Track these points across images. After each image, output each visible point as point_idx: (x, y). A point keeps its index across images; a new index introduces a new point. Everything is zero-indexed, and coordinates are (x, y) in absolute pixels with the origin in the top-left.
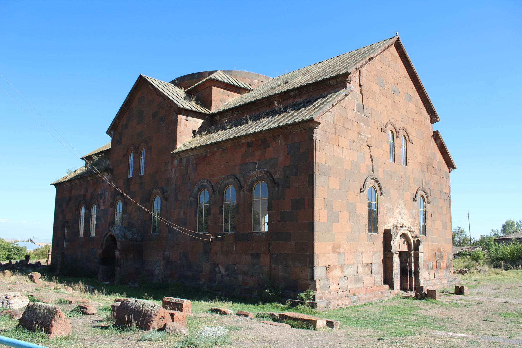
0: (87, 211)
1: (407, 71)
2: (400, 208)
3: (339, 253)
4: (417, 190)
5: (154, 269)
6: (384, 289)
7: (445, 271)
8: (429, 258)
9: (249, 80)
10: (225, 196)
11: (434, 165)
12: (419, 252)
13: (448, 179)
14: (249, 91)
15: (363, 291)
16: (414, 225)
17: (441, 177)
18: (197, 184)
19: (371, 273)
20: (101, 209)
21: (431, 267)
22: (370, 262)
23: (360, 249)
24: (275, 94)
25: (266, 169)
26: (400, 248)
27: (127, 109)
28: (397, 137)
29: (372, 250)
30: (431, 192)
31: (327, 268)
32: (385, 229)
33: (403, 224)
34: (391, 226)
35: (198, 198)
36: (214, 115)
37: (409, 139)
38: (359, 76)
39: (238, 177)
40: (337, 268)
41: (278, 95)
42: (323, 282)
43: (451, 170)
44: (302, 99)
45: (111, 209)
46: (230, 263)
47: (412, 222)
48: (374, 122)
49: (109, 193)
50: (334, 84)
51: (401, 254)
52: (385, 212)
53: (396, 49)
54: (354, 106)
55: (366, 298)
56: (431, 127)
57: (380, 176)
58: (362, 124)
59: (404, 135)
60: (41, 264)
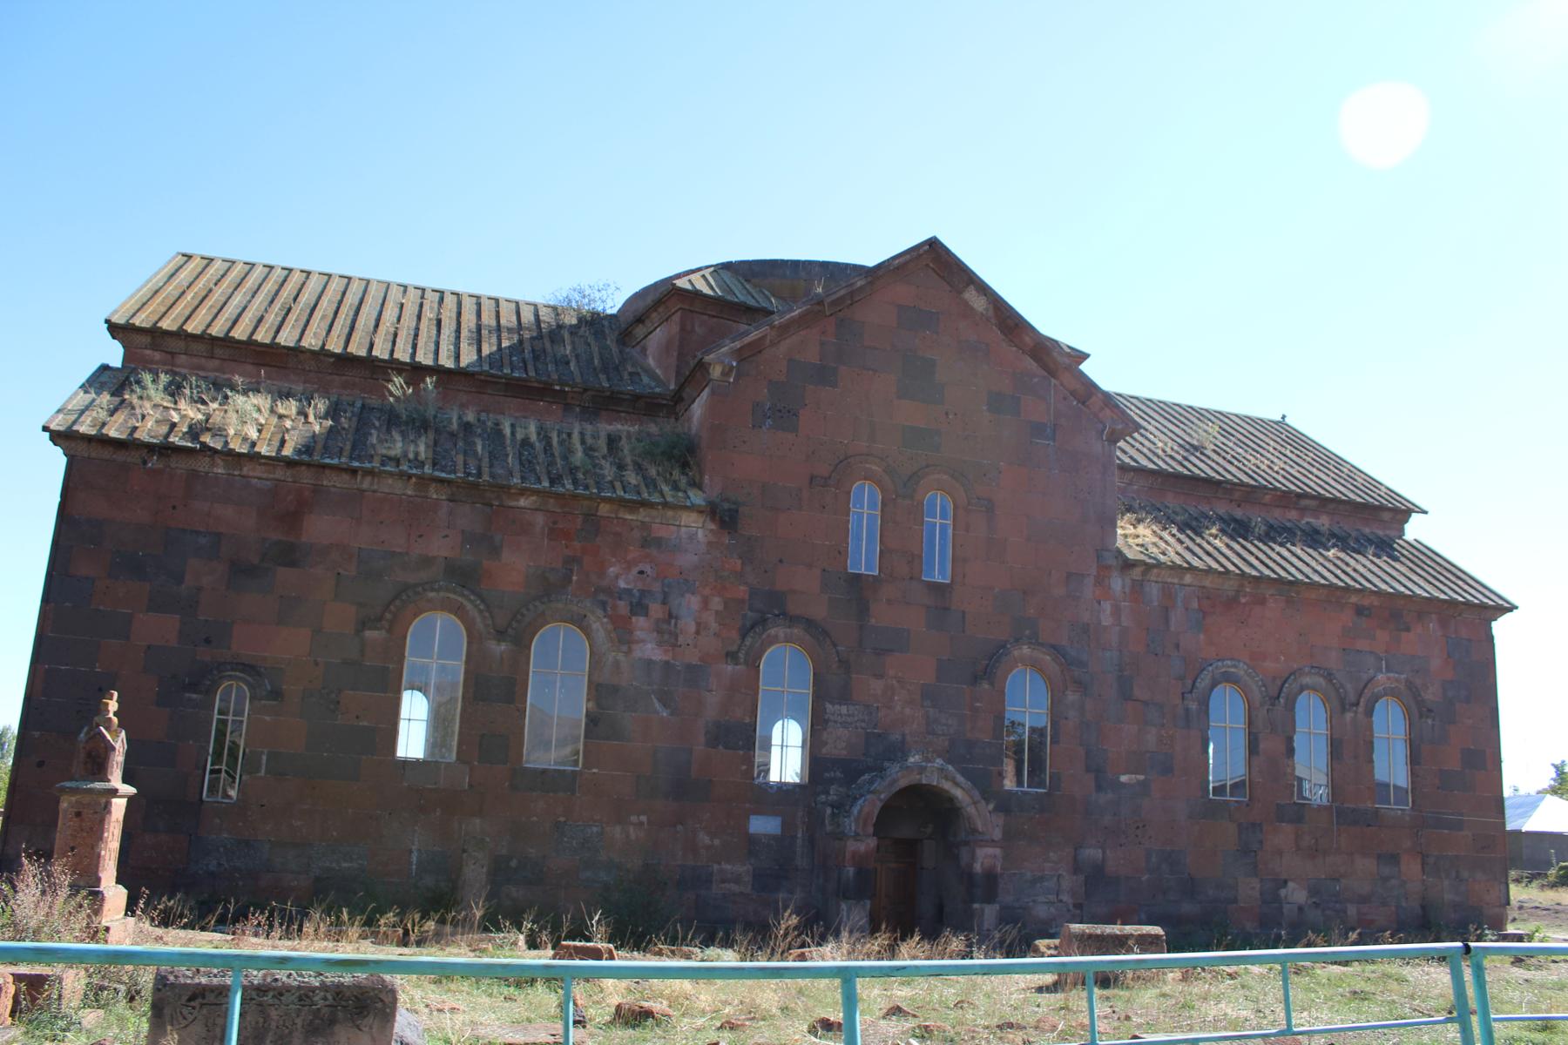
27: (828, 314)
46: (1323, 877)
49: (705, 603)
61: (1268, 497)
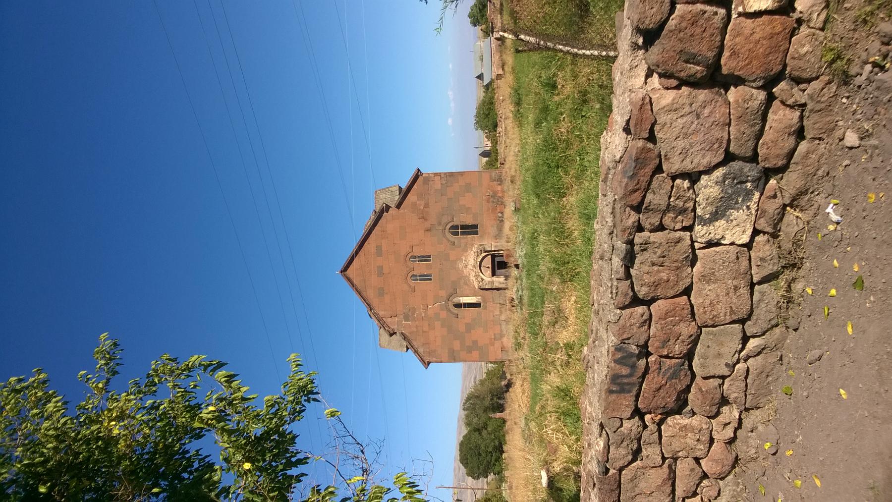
3: (495, 339)
11: (422, 207)
13: (427, 180)
23: (492, 318)
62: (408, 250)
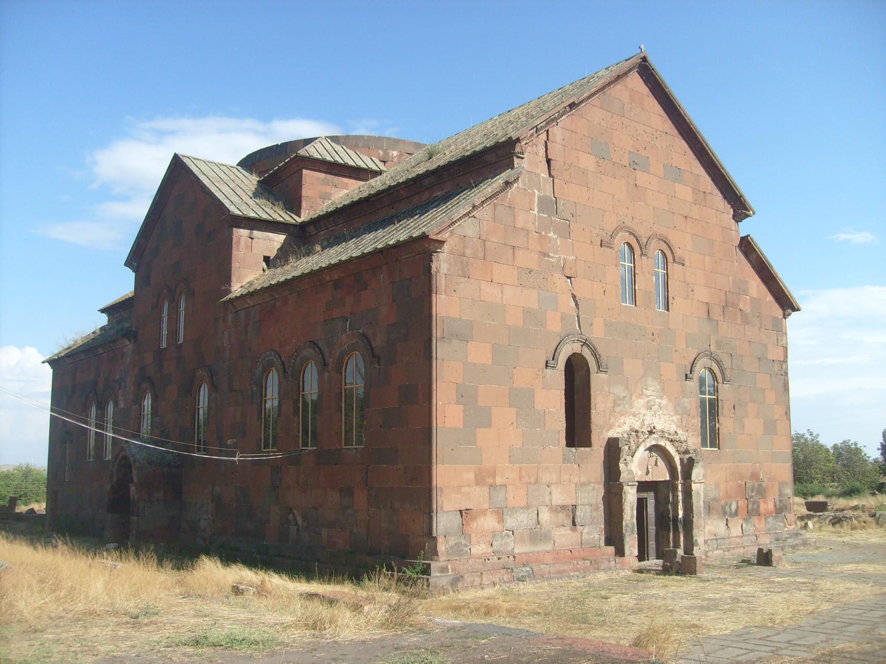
0: (99, 412)
1: (671, 119)
2: (648, 396)
3: (493, 486)
4: (695, 359)
5: (199, 520)
6: (604, 555)
7: (770, 519)
8: (727, 493)
9: (381, 152)
10: (303, 382)
11: (741, 306)
12: (691, 481)
13: (780, 330)
14: (376, 173)
15: (549, 558)
16: (687, 429)
17: (762, 330)
18: (260, 360)
19: (574, 524)
20: (119, 407)
21: (733, 511)
22: (569, 502)
23: (545, 478)
24: (399, 184)
25: (362, 330)
26: (650, 473)
28: (642, 254)
29: (576, 479)
30: (734, 360)
31: (464, 514)
32: (609, 438)
33: (654, 427)
34: (625, 432)
35: (264, 382)
36: (303, 226)
37: (674, 257)
38: (546, 142)
39: (321, 344)
40: (488, 514)
41: (403, 186)
42: (452, 541)
43: (787, 313)
44: (444, 191)
45: (135, 407)
46: (310, 506)
47: (682, 422)
48: (583, 229)
50: (494, 161)
51: (643, 486)
52: (610, 405)
53: (642, 78)
54: (531, 201)
55: (552, 571)
56: (733, 229)
57: (597, 333)
58: (551, 234)
59: (660, 250)
60: (36, 513)
61: (402, 192)
62: (678, 253)
